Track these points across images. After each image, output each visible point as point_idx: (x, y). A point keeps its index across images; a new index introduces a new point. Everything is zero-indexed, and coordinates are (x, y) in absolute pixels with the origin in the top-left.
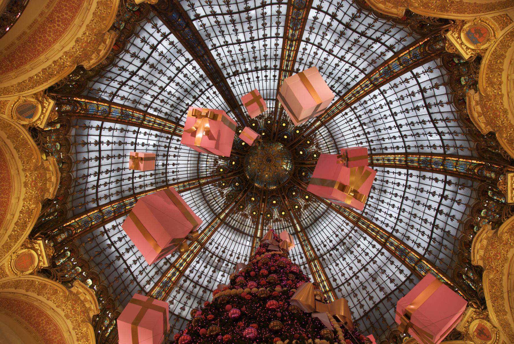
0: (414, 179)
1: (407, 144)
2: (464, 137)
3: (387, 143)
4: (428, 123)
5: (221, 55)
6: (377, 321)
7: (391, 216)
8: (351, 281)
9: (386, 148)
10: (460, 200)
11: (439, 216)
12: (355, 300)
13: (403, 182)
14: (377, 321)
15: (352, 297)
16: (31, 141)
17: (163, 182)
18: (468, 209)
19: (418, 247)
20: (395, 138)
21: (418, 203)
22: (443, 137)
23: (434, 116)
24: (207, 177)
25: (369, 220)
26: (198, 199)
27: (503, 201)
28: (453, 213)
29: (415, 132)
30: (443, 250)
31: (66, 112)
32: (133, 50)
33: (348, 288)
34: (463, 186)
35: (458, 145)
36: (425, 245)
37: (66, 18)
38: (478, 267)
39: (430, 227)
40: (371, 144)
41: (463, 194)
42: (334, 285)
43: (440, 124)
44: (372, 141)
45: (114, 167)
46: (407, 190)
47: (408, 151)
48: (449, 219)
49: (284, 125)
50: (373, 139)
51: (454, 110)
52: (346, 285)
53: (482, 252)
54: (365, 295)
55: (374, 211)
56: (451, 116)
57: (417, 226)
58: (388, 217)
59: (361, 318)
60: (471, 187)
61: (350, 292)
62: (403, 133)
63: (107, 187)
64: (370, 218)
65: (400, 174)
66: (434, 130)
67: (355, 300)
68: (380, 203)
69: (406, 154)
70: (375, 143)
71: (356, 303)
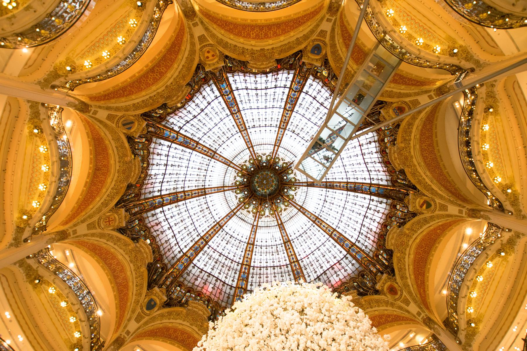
2: (384, 173)
5: (247, 116)
12: (312, 268)
16: (127, 145)
17: (203, 186)
18: (384, 216)
24: (229, 187)
25: (322, 220)
30: (367, 240)
31: (151, 132)
32: (197, 101)
34: (381, 203)
37: (162, 72)
38: (389, 250)
43: (370, 165)
45: (175, 172)
49: (277, 160)
53: (393, 241)
54: (318, 265)
60: (386, 203)
63: (168, 184)
64: (323, 219)
67: (312, 268)
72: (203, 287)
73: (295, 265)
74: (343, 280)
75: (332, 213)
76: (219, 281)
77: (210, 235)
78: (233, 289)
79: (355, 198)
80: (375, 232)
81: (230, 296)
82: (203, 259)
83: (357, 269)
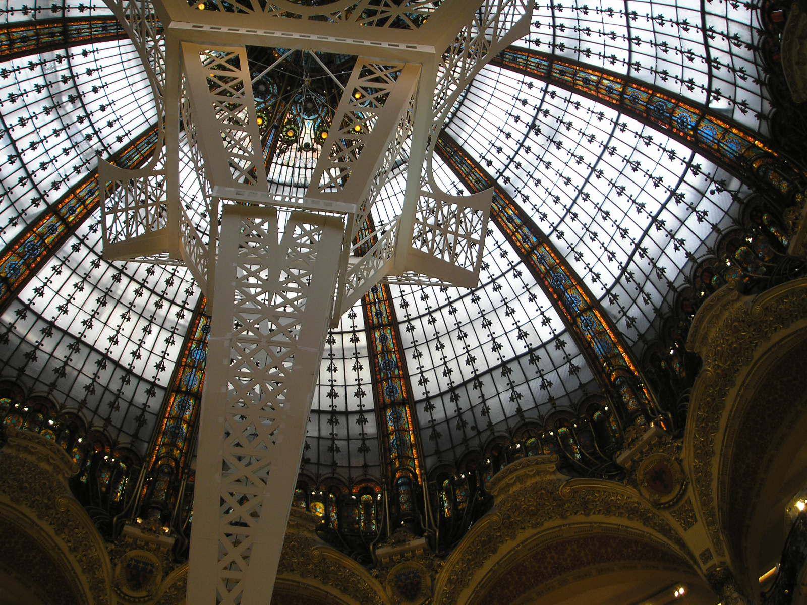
0: (628, 137)
1: (636, 58)
2: (756, 88)
3: (593, 43)
4: (693, 30)
6: (472, 408)
7: (557, 200)
8: (437, 315)
9: (588, 53)
10: (705, 213)
11: (653, 231)
12: (437, 355)
13: (602, 137)
14: (472, 408)
15: (433, 348)
19: (594, 280)
20: (613, 36)
21: (621, 191)
22: (714, 70)
23: (711, 21)
26: (133, 63)
27: (785, 243)
28: (682, 234)
29: (660, 39)
30: (640, 301)
33: (429, 328)
34: (723, 186)
35: (739, 100)
36: (610, 282)
39: (630, 249)
40: (558, 32)
41: (717, 204)
42: (400, 314)
43: (718, 42)
44: (562, 27)
46: (606, 156)
47: (634, 73)
48: (672, 245)
50: (567, 23)
51: (755, 24)
52: (425, 320)
54: (460, 351)
55: (525, 179)
56: (745, 35)
57: (603, 237)
58: (550, 200)
59: (441, 395)
61: (430, 336)
62: (634, 33)
65: (601, 116)
66: (700, 50)
67: (437, 355)
68: (542, 167)
69: (627, 80)
70: (567, 32)
71: (437, 362)
72: (53, 385)
73: (383, 339)
74: (526, 415)
75: (548, 177)
76: (110, 367)
77: (82, 201)
78: (160, 394)
79: (642, 146)
80: (670, 284)
81: (147, 416)
82: (56, 285)
83: (581, 386)
